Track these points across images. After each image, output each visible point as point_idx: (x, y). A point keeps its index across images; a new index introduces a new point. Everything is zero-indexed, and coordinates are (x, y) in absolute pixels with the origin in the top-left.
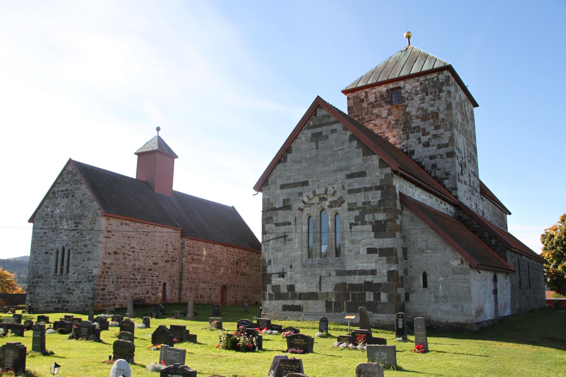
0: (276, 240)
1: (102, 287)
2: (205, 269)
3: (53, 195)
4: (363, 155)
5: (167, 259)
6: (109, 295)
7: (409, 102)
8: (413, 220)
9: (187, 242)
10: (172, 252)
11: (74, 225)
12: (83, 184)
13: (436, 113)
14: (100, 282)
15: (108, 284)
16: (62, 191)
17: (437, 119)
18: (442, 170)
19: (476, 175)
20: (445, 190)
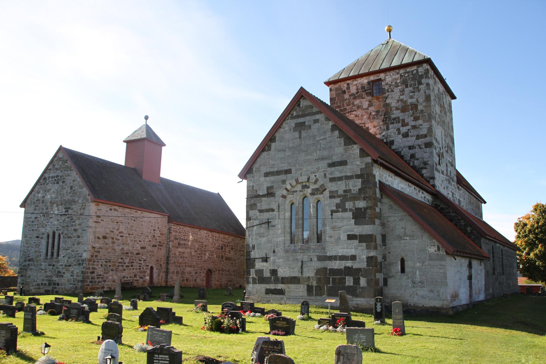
0: (260, 226)
1: (91, 270)
2: (191, 254)
3: (45, 181)
4: (345, 145)
5: (154, 243)
6: (98, 278)
7: (389, 93)
8: (392, 208)
9: (174, 227)
10: (159, 237)
11: (64, 211)
12: (73, 170)
13: (415, 104)
14: (89, 265)
15: (97, 267)
16: (52, 177)
18: (420, 160)
19: (453, 165)
20: (423, 180)
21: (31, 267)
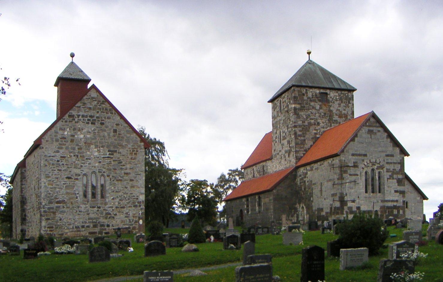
11: (108, 153)
16: (83, 116)
17: (347, 119)
21: (63, 209)
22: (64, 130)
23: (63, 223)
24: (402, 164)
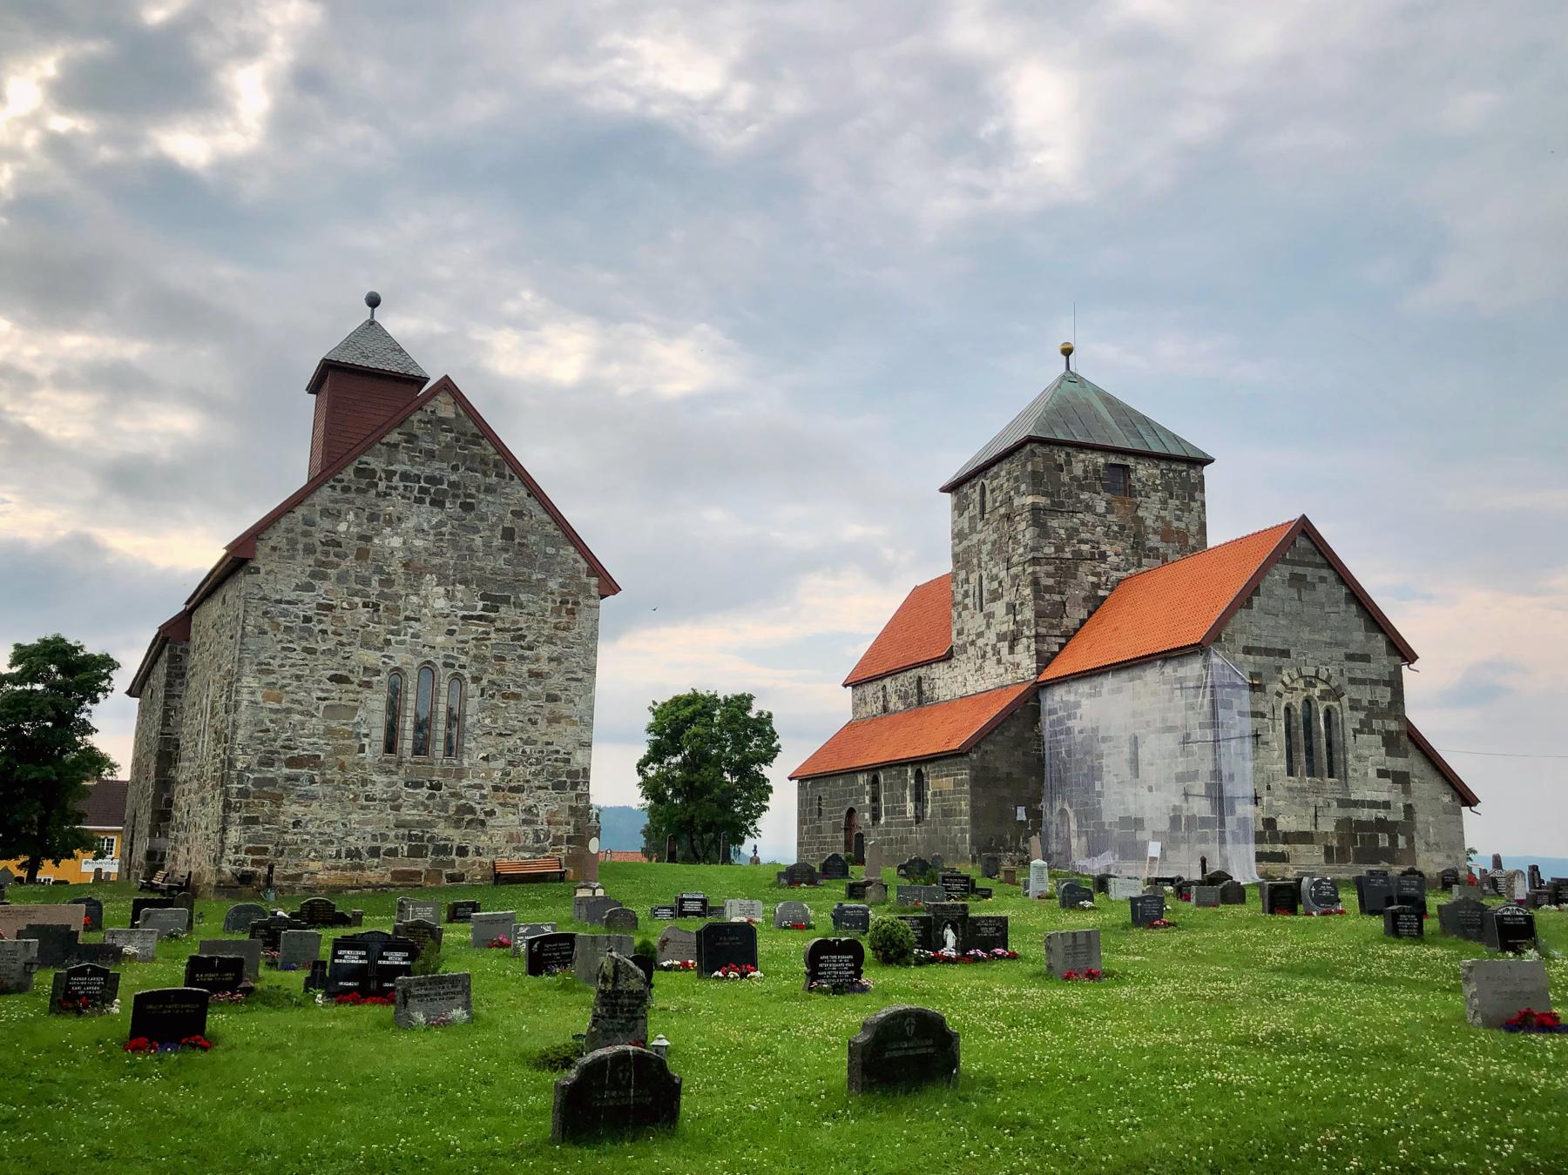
11: (480, 604)
12: (512, 478)
16: (405, 476)
21: (307, 788)
22: (337, 516)
23: (306, 837)
24: (1396, 685)
